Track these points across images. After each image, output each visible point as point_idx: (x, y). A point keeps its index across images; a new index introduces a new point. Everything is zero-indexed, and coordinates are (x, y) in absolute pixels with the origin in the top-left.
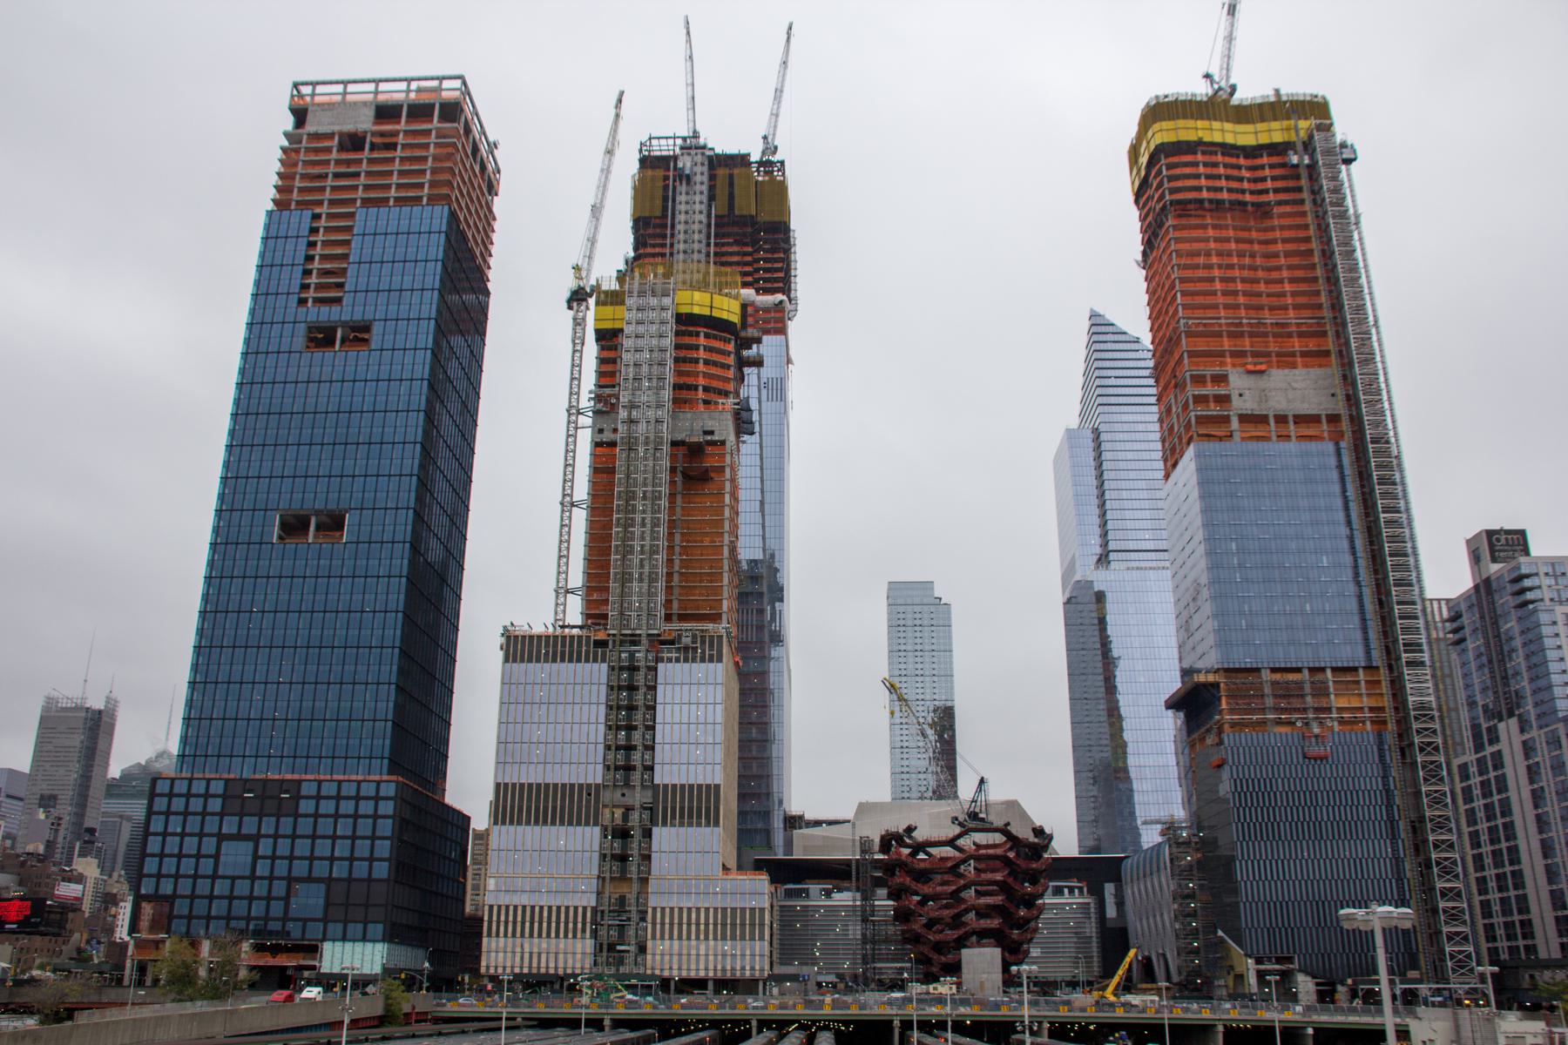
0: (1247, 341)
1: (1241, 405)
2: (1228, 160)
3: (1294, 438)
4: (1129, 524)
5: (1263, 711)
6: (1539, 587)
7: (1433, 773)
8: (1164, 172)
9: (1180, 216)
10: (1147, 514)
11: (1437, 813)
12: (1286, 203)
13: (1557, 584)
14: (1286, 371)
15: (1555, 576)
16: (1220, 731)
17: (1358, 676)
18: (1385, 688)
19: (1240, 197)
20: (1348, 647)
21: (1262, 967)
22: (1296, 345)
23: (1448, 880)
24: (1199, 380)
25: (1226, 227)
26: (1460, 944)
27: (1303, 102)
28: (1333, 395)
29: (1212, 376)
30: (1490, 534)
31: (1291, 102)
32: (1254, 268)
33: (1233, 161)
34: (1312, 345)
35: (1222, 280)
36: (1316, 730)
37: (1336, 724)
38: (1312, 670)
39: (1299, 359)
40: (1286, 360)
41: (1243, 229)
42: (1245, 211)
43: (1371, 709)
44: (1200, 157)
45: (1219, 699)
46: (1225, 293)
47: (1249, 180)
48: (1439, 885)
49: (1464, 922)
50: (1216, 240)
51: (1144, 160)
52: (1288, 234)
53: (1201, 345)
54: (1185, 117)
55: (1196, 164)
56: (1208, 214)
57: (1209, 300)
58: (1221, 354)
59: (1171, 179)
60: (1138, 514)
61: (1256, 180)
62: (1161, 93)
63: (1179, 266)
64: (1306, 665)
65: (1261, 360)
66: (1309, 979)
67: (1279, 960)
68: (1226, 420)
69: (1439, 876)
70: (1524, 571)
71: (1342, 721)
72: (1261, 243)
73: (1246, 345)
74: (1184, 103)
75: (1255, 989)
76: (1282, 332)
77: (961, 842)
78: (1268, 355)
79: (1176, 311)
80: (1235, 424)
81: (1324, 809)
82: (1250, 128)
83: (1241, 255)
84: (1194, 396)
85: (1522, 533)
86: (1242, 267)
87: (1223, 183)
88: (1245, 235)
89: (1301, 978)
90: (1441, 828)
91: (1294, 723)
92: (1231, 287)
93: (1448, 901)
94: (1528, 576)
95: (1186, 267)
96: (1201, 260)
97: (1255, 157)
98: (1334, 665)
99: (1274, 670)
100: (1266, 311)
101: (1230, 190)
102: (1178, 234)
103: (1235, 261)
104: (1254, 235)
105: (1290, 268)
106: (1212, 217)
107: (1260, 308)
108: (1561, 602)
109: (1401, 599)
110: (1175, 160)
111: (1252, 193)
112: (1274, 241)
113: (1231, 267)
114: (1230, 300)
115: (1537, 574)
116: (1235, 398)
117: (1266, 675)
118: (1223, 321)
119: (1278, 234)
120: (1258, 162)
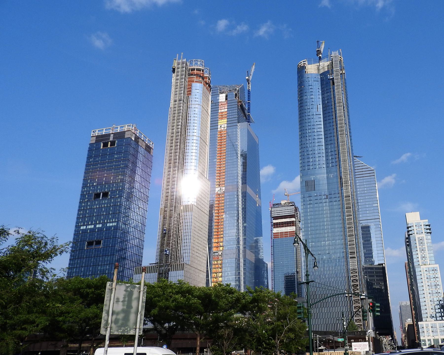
20: (339, 254)
93: (357, 322)
94: (411, 227)
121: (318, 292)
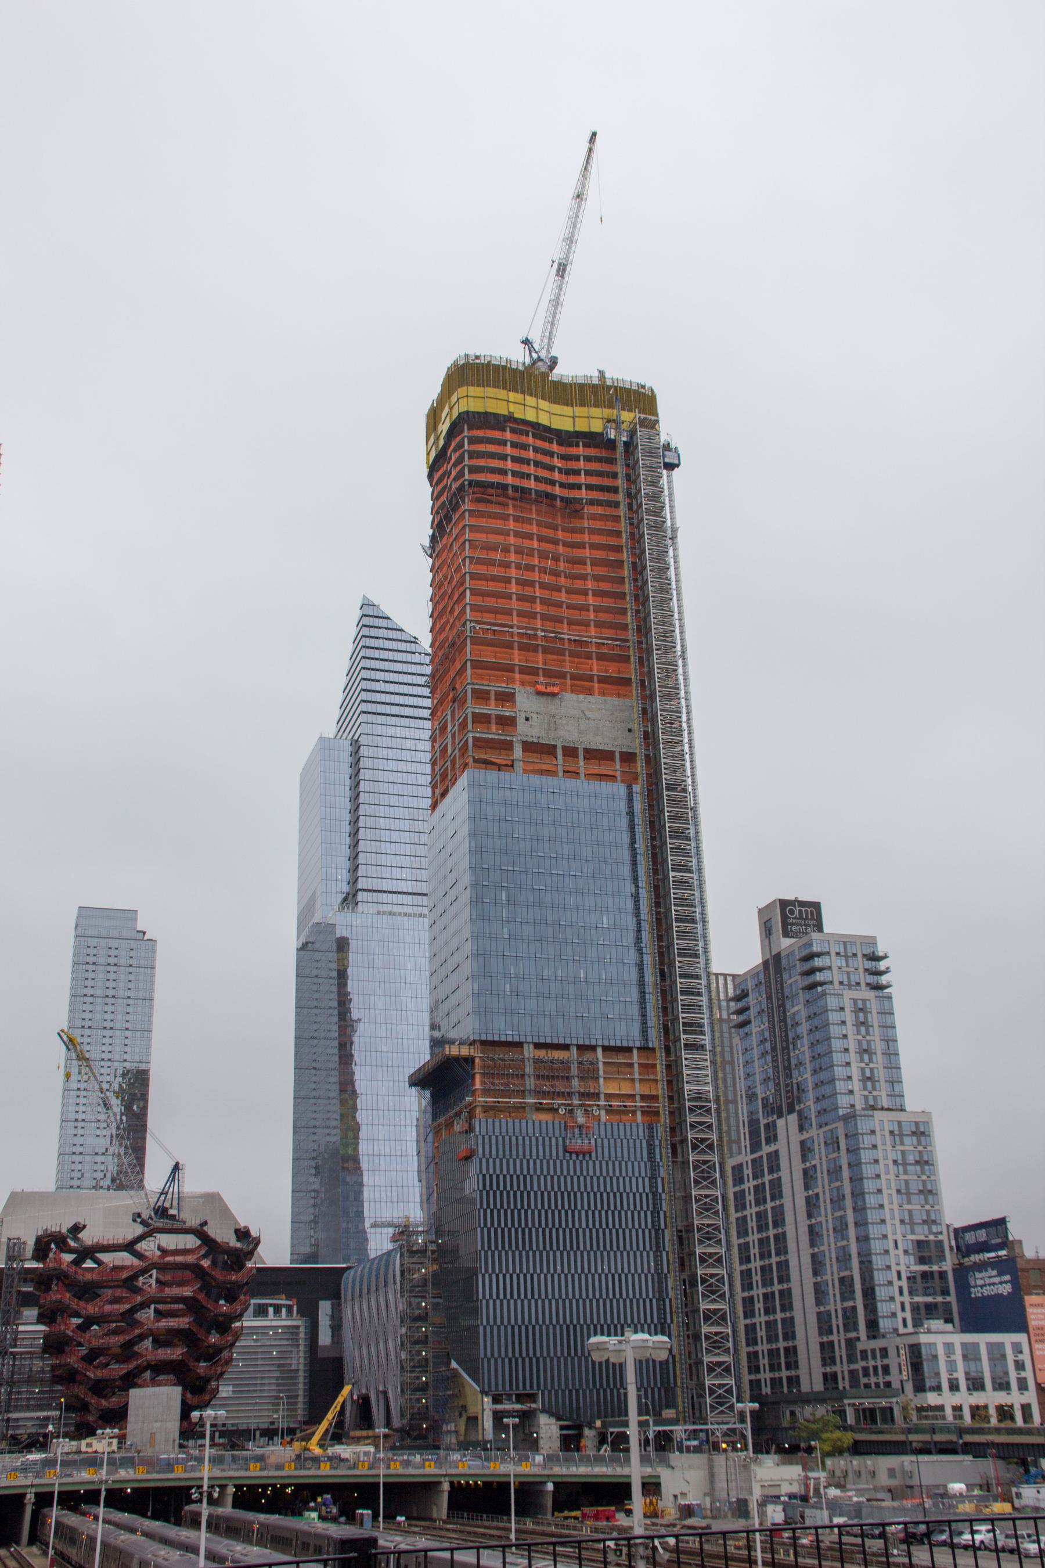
0: (540, 657)
1: (527, 731)
2: (539, 444)
3: (582, 776)
4: (385, 860)
5: (522, 1093)
6: (830, 968)
7: (705, 1177)
8: (466, 447)
9: (478, 501)
10: (407, 849)
11: (706, 1221)
12: (599, 503)
13: (847, 965)
14: (581, 697)
15: (846, 957)
16: (471, 1116)
17: (632, 1058)
18: (660, 1073)
19: (548, 489)
21: (500, 1407)
22: (595, 668)
23: (714, 1301)
24: (481, 696)
25: (529, 521)
26: (722, 1376)
27: (628, 391)
28: (630, 730)
29: (497, 693)
30: (784, 904)
31: (616, 388)
32: (556, 574)
33: (546, 445)
34: (612, 670)
35: (520, 582)
36: (581, 1120)
37: (603, 1112)
38: (581, 1048)
39: (596, 685)
40: (582, 684)
41: (549, 526)
42: (553, 506)
43: (644, 1097)
44: (508, 436)
45: (473, 1078)
46: (521, 598)
47: (560, 471)
48: (704, 1306)
49: (727, 1351)
50: (517, 534)
51: (444, 427)
52: (598, 539)
53: (488, 655)
54: (496, 386)
55: (503, 443)
56: (511, 502)
57: (502, 604)
58: (510, 669)
59: (472, 455)
60: (396, 848)
61: (568, 472)
62: (472, 353)
63: (471, 558)
64: (574, 1042)
65: (553, 681)
66: (553, 1421)
67: (520, 1398)
68: (508, 746)
69: (703, 1295)
70: (816, 948)
71: (610, 1110)
72: (566, 545)
73: (539, 660)
74: (497, 368)
75: (489, 1435)
76: (580, 651)
77: (142, 1246)
78: (562, 676)
79: (463, 612)
80: (518, 752)
81: (583, 1213)
82: (568, 410)
83: (544, 555)
84: (474, 714)
85: (816, 906)
86: (543, 570)
87: (531, 470)
88: (550, 533)
89: (544, 1420)
90: (709, 1239)
91: (557, 1110)
92: (528, 591)
93: (712, 1324)
94: (819, 955)
95: (480, 562)
96: (498, 556)
97: (570, 445)
98: (606, 1043)
99: (538, 1046)
100: (565, 625)
101: (537, 479)
102: (474, 522)
103: (536, 561)
104: (560, 535)
105: (596, 578)
106: (514, 506)
107: (559, 620)
108: (850, 986)
109: (685, 971)
110: (480, 433)
111: (562, 485)
112: (581, 546)
113: (530, 568)
114: (526, 607)
115: (828, 953)
116: (520, 721)
117: (529, 1052)
118: (515, 630)
119: (586, 538)
120: (573, 451)
121: (535, 1178)
